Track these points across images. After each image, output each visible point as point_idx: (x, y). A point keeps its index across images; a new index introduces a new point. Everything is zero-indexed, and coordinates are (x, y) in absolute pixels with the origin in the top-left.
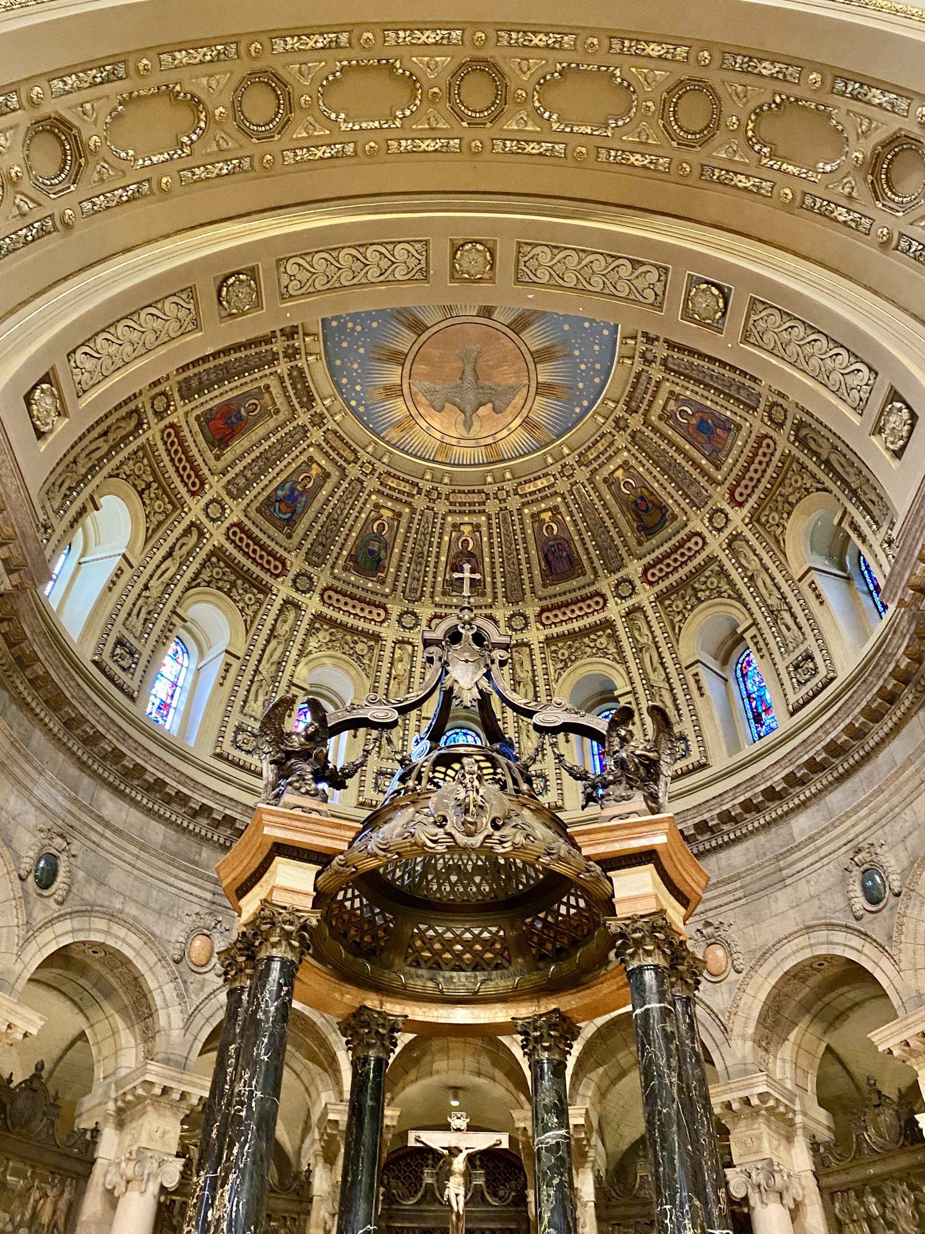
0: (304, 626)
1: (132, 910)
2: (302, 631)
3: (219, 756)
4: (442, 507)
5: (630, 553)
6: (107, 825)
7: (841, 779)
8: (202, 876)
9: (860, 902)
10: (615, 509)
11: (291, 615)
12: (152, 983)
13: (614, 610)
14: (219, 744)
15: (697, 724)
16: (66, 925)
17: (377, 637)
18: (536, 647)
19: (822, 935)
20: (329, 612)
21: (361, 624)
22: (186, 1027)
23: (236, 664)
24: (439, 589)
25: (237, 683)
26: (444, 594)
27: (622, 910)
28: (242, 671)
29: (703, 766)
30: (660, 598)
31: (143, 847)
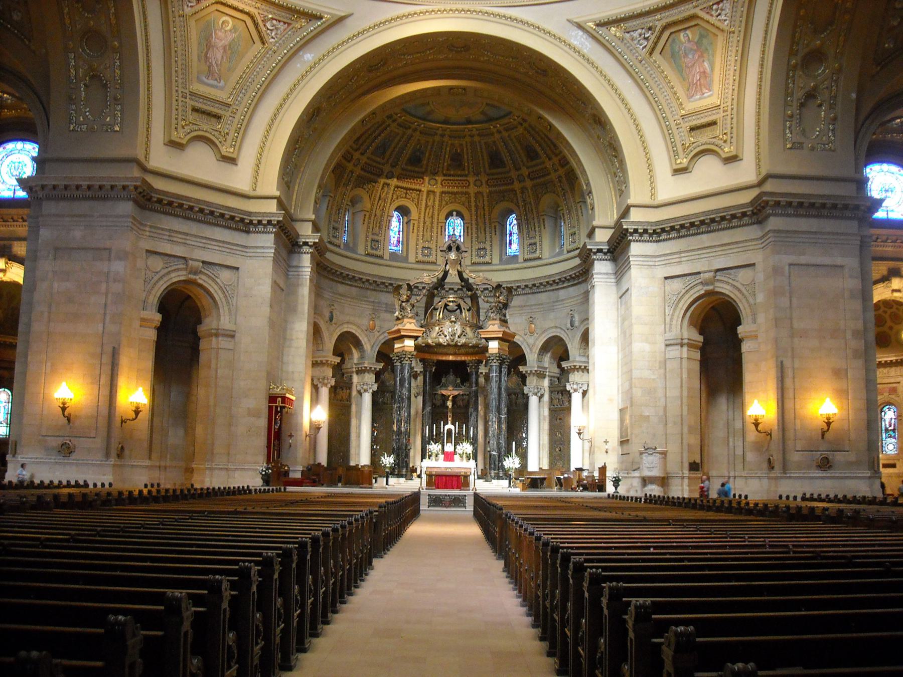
0: (392, 192)
1: (352, 319)
2: (391, 194)
3: (368, 255)
4: (446, 139)
5: (524, 165)
6: (340, 295)
7: (573, 285)
8: (369, 302)
9: (569, 325)
10: (519, 148)
11: (386, 189)
12: (361, 339)
13: (517, 186)
14: (366, 250)
15: (541, 241)
16: (339, 329)
17: (420, 191)
18: (485, 194)
19: (559, 330)
20: (400, 184)
21: (413, 186)
22: (372, 350)
23: (368, 214)
24: (445, 168)
25: (369, 223)
26: (448, 170)
27: (490, 351)
28: (370, 218)
29: (539, 258)
30: (534, 186)
31: (352, 298)
